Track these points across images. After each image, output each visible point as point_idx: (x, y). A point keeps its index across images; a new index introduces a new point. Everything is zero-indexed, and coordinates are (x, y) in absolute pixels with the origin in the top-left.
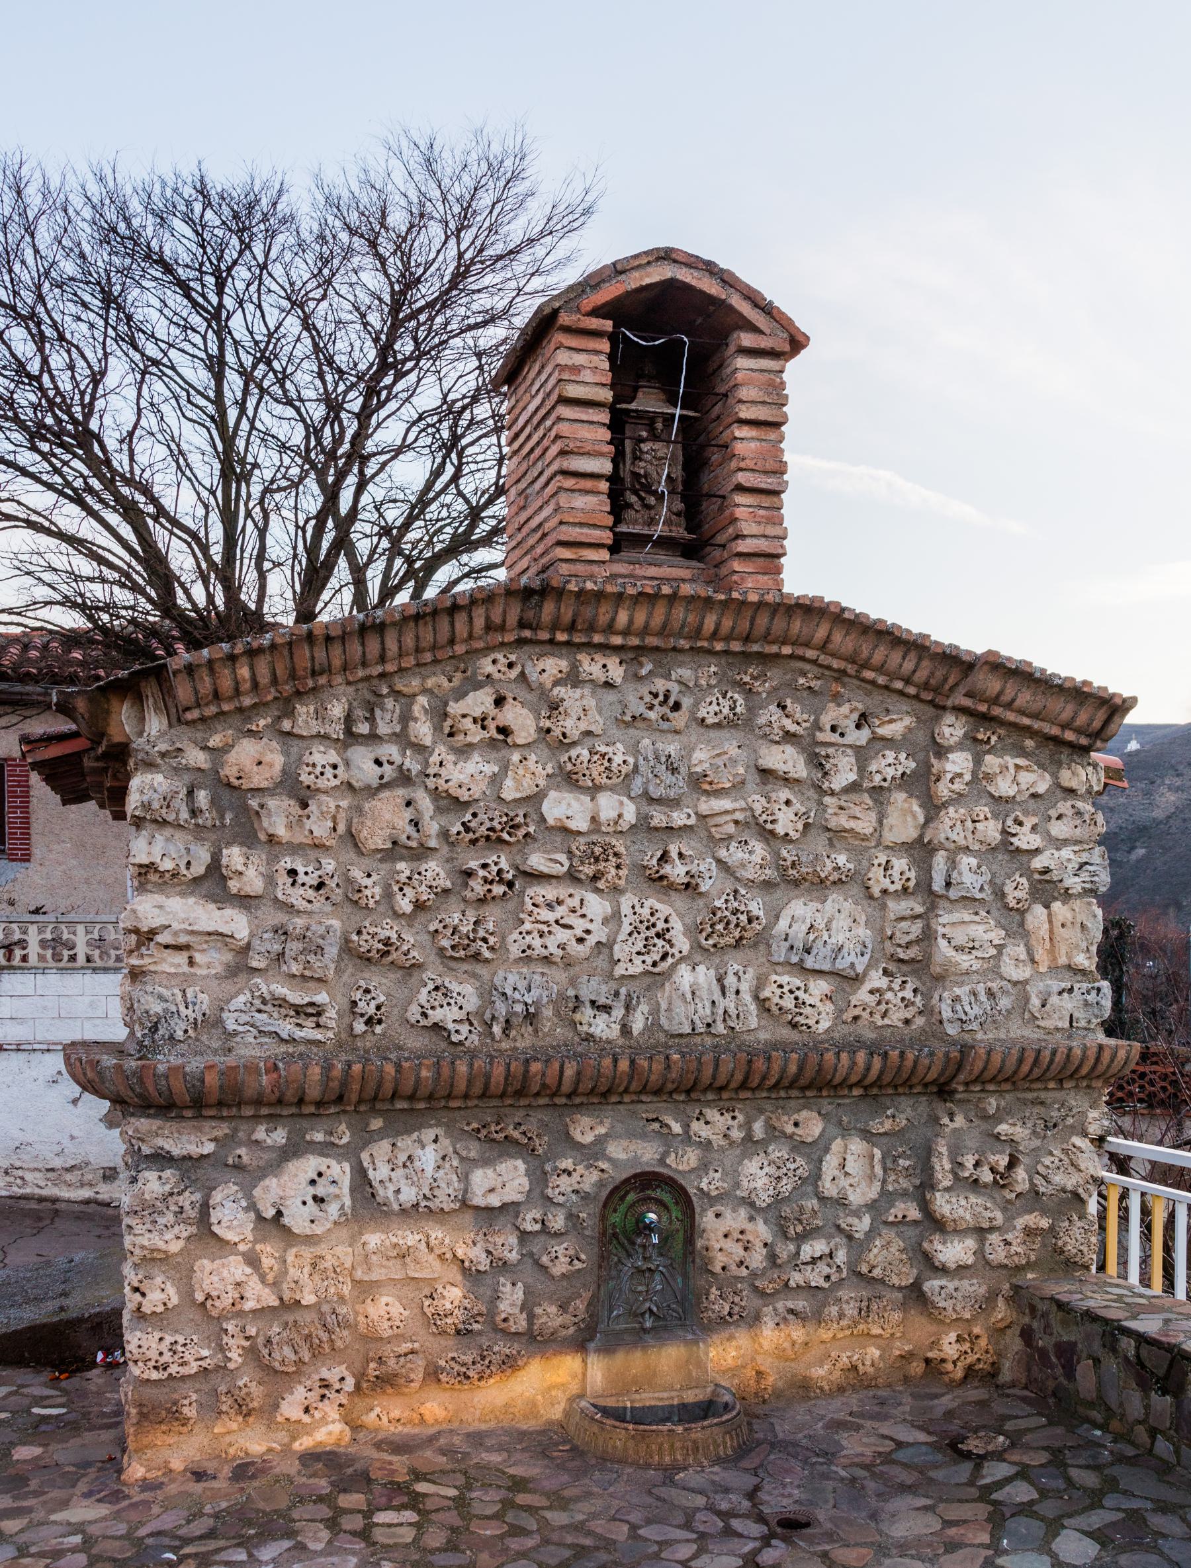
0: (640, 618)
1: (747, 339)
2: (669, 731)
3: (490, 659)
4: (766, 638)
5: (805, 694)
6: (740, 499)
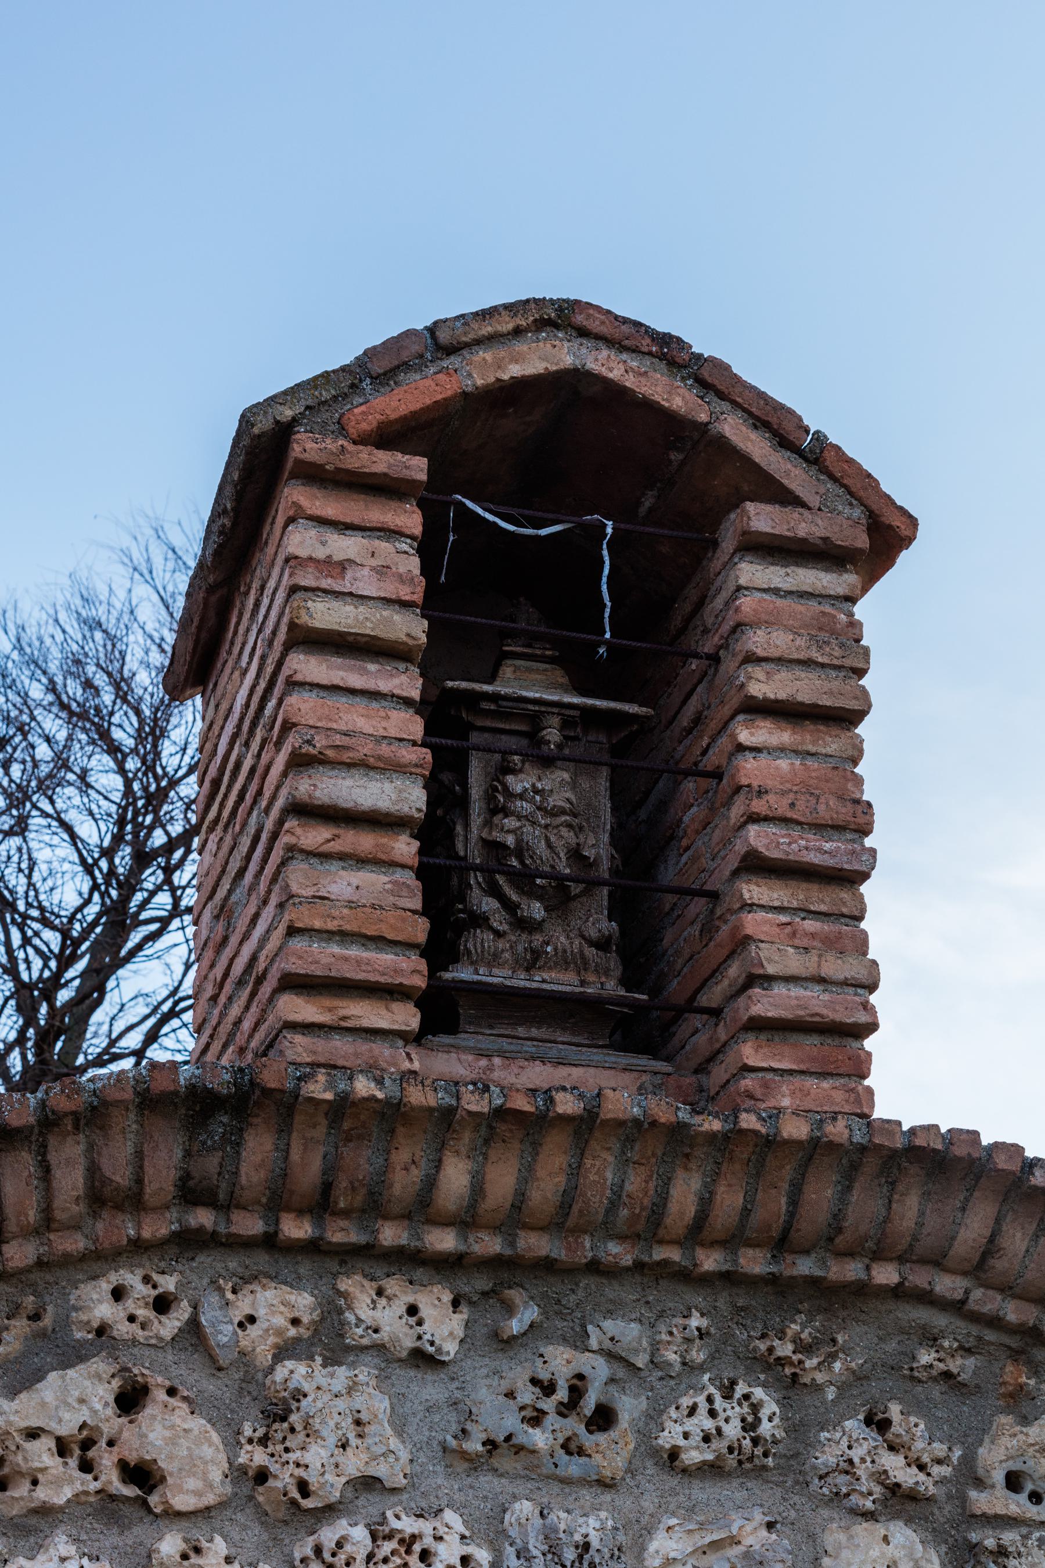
0: (502, 1180)
1: (762, 518)
2: (584, 1482)
3: (105, 1286)
4: (832, 1240)
5: (936, 1391)
6: (753, 890)
